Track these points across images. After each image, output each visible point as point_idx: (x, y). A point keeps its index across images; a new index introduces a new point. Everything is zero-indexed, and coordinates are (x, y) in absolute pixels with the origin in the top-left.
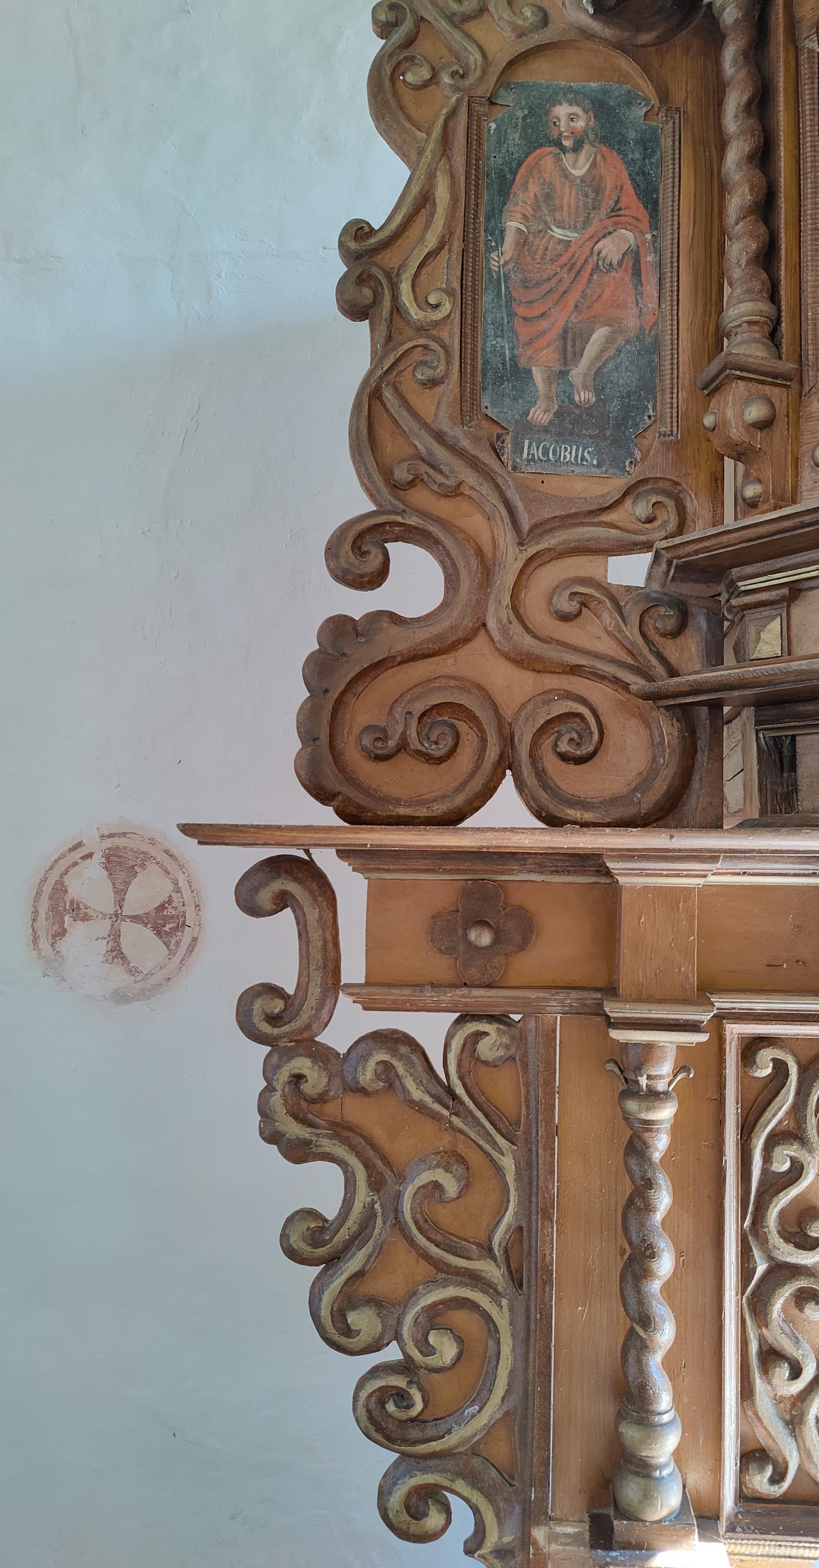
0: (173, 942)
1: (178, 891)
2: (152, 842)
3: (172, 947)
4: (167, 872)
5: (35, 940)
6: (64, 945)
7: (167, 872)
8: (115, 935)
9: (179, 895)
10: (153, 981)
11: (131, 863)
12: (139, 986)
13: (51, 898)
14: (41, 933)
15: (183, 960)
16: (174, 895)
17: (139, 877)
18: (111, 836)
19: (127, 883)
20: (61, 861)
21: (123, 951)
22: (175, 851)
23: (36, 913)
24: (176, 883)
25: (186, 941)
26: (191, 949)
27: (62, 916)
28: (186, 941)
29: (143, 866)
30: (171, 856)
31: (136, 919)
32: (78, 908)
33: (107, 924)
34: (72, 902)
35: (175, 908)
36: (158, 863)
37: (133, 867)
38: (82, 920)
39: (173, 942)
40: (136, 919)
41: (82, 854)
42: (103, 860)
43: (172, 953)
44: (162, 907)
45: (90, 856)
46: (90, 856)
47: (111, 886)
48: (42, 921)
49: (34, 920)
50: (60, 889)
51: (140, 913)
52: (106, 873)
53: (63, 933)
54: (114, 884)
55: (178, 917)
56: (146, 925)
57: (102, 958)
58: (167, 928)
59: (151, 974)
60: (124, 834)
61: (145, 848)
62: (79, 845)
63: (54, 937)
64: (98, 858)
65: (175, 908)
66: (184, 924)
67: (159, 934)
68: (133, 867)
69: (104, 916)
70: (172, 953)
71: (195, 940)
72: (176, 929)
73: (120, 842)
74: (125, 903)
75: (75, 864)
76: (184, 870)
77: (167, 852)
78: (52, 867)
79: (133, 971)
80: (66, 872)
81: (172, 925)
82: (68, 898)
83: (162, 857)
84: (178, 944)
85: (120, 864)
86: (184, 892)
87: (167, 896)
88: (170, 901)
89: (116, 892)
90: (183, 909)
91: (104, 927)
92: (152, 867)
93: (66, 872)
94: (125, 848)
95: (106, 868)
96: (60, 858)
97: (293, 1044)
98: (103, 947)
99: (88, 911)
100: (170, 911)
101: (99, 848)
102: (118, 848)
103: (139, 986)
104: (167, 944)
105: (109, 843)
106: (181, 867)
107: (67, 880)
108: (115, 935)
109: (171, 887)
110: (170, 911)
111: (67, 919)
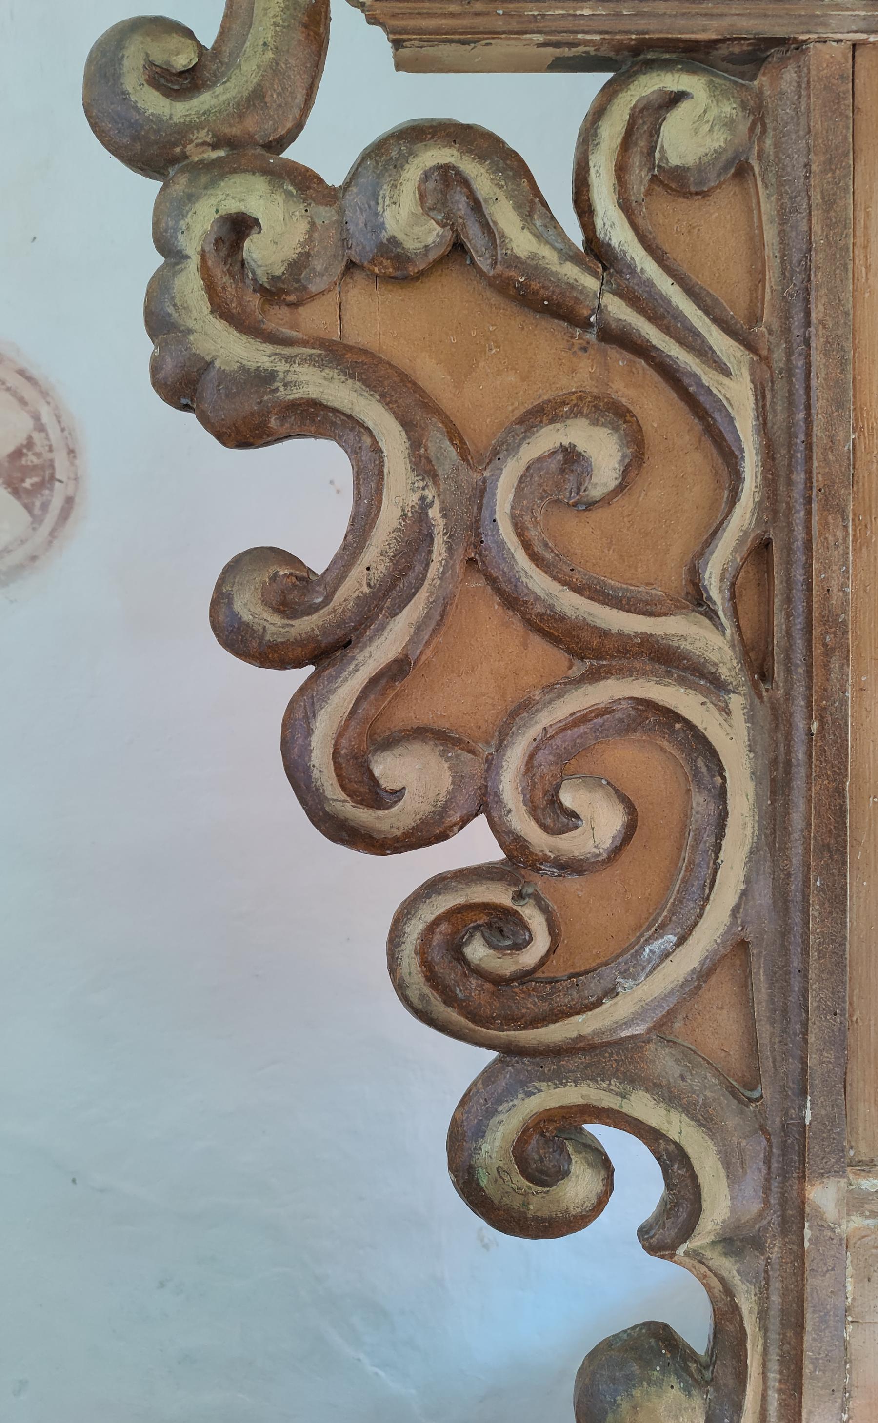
0: (38, 504)
1: (41, 428)
3: (37, 511)
4: (23, 402)
7: (23, 402)
9: (43, 435)
16: (37, 437)
22: (34, 372)
24: (37, 418)
25: (57, 503)
28: (57, 503)
30: (30, 379)
35: (38, 455)
36: (8, 389)
39: (38, 504)
43: (37, 521)
44: (18, 454)
55: (42, 468)
58: (28, 483)
65: (38, 455)
66: (52, 478)
67: (16, 492)
70: (37, 521)
71: (69, 501)
76: (49, 399)
77: (22, 373)
81: (35, 480)
84: (45, 507)
86: (50, 431)
87: (25, 436)
88: (30, 444)
90: (49, 456)
97: (222, 153)
100: (30, 459)
104: (28, 508)
106: (45, 394)
109: (30, 423)
110: (30, 459)
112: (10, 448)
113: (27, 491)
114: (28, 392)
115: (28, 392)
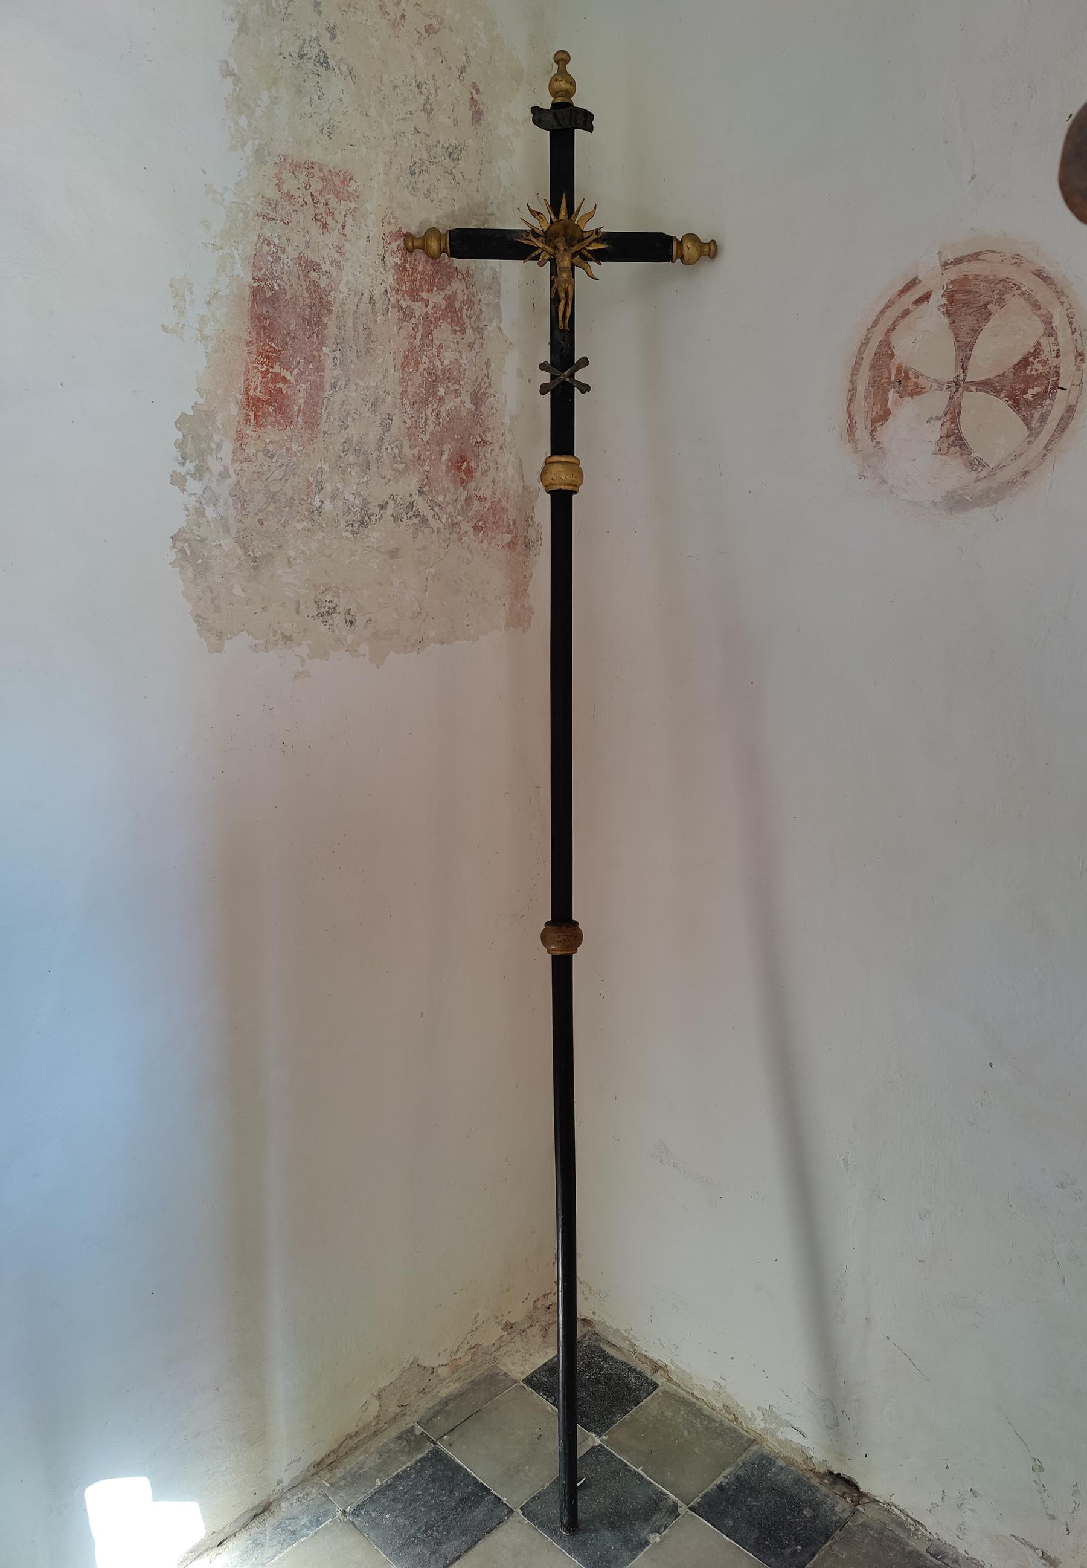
0: (1037, 415)
1: (1051, 333)
2: (1017, 260)
3: (1035, 424)
4: (1036, 306)
5: (851, 429)
6: (888, 432)
7: (1036, 306)
8: (954, 413)
9: (1052, 340)
10: (1003, 476)
11: (983, 300)
12: (982, 485)
13: (872, 367)
14: (859, 419)
15: (1049, 442)
16: (1044, 342)
17: (994, 320)
18: (958, 261)
19: (976, 332)
20: (888, 312)
21: (964, 434)
22: (1051, 271)
23: (853, 390)
26: (1063, 425)
27: (885, 392)
29: (1001, 302)
31: (984, 385)
32: (907, 377)
33: (945, 395)
34: (899, 370)
35: (1044, 362)
36: (1023, 294)
37: (985, 306)
38: (911, 395)
39: (1037, 415)
40: (984, 385)
41: (916, 297)
42: (944, 301)
43: (1033, 433)
44: (1025, 363)
45: (926, 297)
46: (926, 297)
47: (952, 338)
48: (861, 403)
49: (851, 401)
50: (886, 352)
51: (991, 375)
52: (946, 321)
53: (884, 416)
54: (956, 336)
55: (1047, 376)
56: (997, 393)
57: (933, 447)
58: (1029, 396)
59: (1000, 467)
60: (976, 256)
61: (1007, 271)
62: (913, 283)
63: (874, 422)
64: (938, 299)
66: (1056, 386)
67: (1016, 405)
68: (985, 306)
69: (941, 384)
70: (1033, 433)
71: (1071, 409)
72: (1044, 395)
73: (969, 269)
74: (971, 365)
75: (906, 313)
76: (1063, 299)
77: (1039, 274)
78: (876, 323)
79: (975, 465)
80: (893, 328)
81: (1038, 389)
82: (896, 361)
83: (1030, 283)
84: (1043, 419)
85: (967, 304)
86: (1060, 334)
87: (1033, 343)
88: (1037, 352)
89: (959, 348)
90: (1054, 362)
91: (937, 402)
92: (1014, 302)
93: (893, 328)
94: (976, 277)
95: (948, 313)
96: (887, 307)
98: (935, 431)
99: (921, 381)
100: (1037, 367)
101: (936, 281)
102: (966, 279)
103: (982, 485)
104: (1027, 421)
105: (952, 274)
106: (1060, 294)
107: (894, 339)
108: (954, 413)
109: (1040, 328)
110: (1037, 367)
111: (892, 395)
112: (1017, 359)
113: (1028, 403)
114: (1043, 294)
115: (1043, 294)
